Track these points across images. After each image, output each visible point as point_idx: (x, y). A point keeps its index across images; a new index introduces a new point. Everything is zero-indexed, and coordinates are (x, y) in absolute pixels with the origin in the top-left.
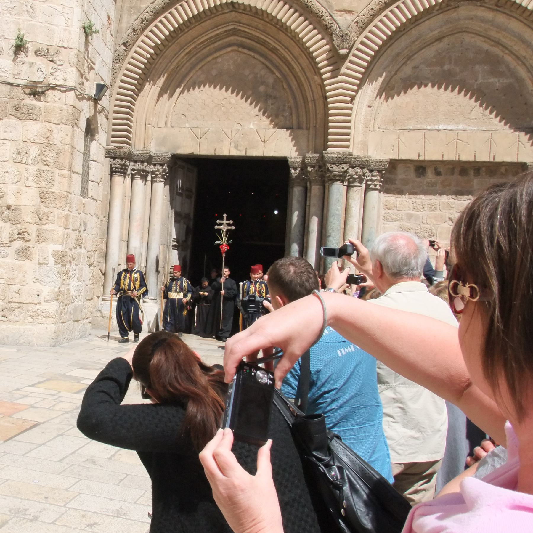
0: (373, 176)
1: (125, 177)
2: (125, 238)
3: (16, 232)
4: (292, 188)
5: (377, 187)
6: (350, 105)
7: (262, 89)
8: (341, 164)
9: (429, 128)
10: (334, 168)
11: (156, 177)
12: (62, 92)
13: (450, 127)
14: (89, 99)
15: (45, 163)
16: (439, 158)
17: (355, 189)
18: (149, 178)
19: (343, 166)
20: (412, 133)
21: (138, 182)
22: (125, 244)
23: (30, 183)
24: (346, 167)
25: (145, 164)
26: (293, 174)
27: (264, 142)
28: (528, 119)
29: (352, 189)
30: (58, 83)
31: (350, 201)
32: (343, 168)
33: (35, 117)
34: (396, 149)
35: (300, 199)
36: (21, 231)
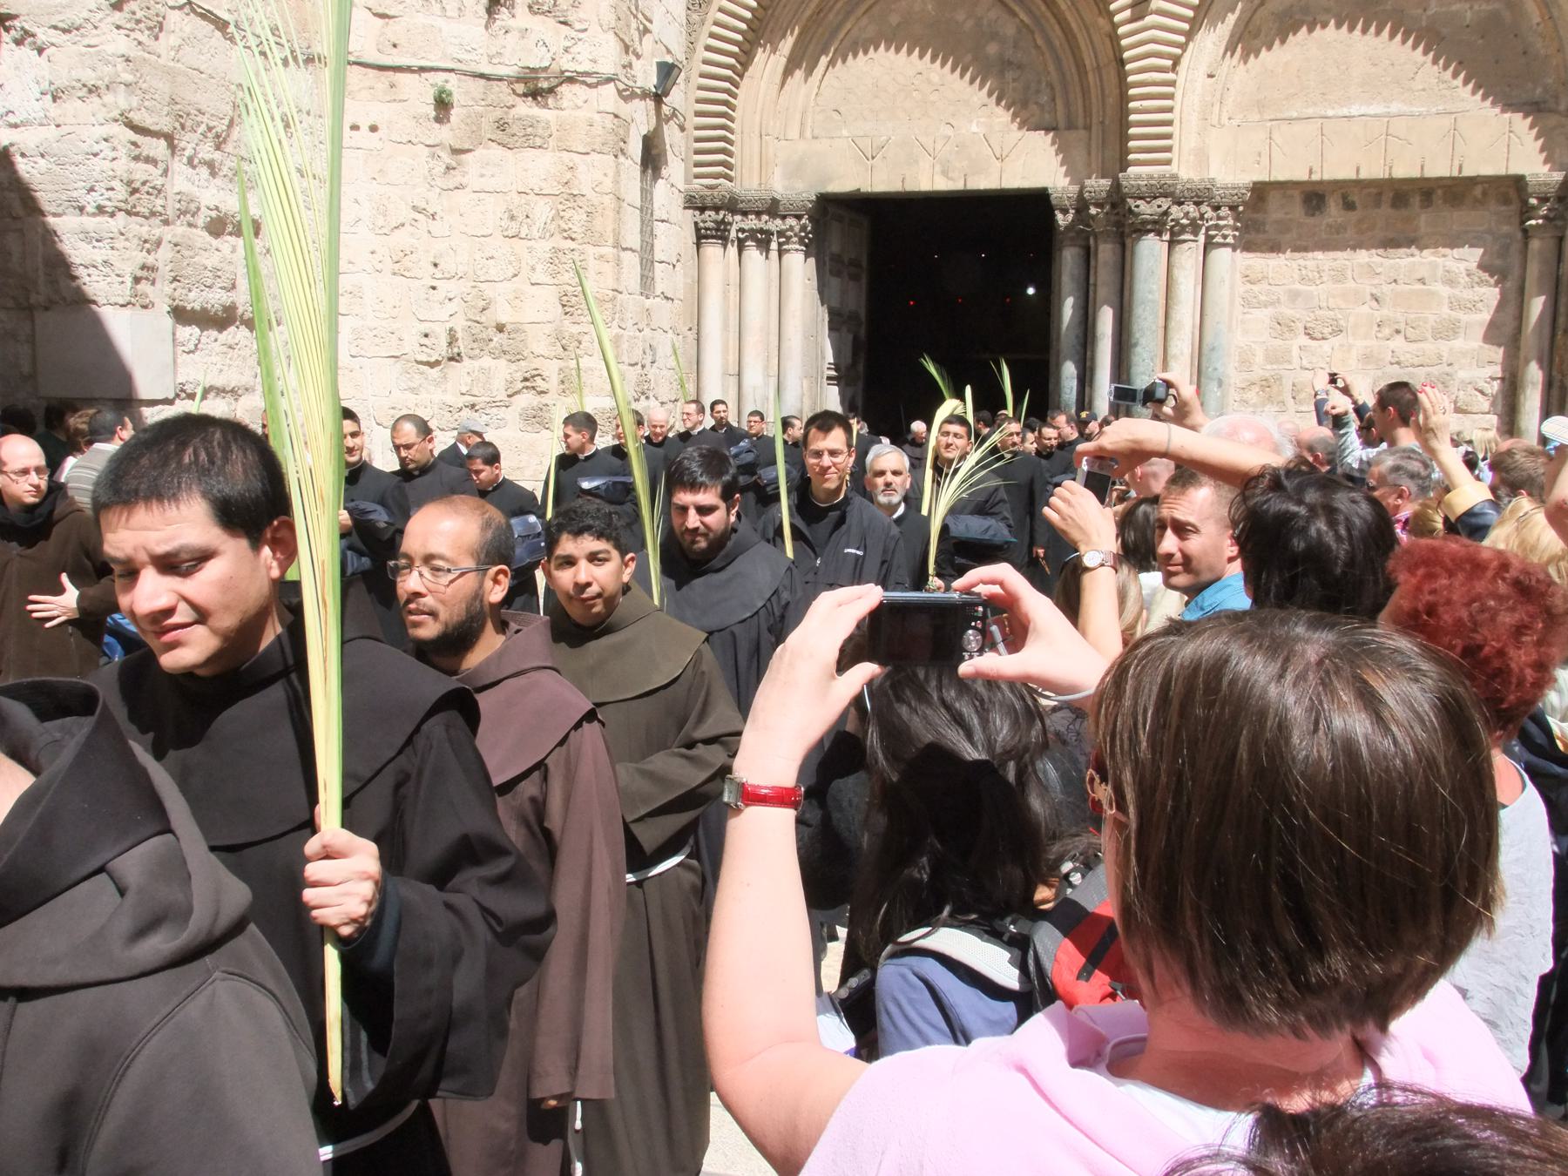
0: (1219, 218)
1: (725, 247)
2: (733, 369)
3: (519, 376)
4: (1060, 250)
5: (1228, 240)
6: (1170, 76)
7: (992, 49)
8: (1155, 198)
9: (1330, 113)
10: (1142, 207)
11: (787, 243)
12: (590, 86)
13: (1372, 110)
14: (645, 95)
15: (565, 234)
16: (1353, 176)
17: (1185, 246)
18: (774, 246)
19: (1158, 201)
20: (1297, 127)
21: (753, 254)
22: (733, 381)
23: (539, 276)
24: (1165, 203)
25: (765, 217)
26: (1061, 222)
27: (1001, 159)
28: (1530, 85)
29: (1178, 248)
30: (580, 69)
31: (1176, 272)
32: (1159, 206)
33: (538, 142)
34: (1264, 160)
35: (1076, 272)
36: (528, 375)
